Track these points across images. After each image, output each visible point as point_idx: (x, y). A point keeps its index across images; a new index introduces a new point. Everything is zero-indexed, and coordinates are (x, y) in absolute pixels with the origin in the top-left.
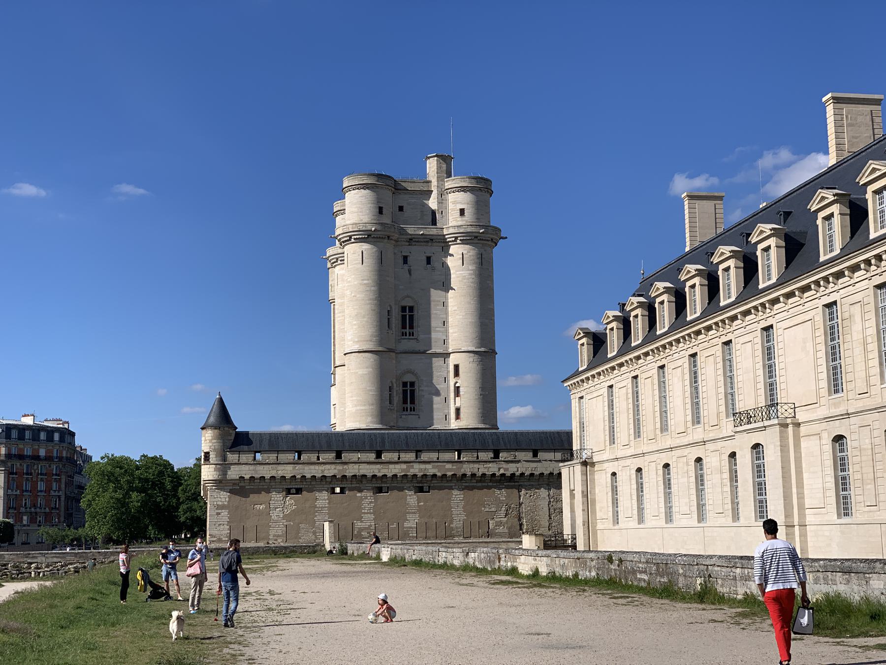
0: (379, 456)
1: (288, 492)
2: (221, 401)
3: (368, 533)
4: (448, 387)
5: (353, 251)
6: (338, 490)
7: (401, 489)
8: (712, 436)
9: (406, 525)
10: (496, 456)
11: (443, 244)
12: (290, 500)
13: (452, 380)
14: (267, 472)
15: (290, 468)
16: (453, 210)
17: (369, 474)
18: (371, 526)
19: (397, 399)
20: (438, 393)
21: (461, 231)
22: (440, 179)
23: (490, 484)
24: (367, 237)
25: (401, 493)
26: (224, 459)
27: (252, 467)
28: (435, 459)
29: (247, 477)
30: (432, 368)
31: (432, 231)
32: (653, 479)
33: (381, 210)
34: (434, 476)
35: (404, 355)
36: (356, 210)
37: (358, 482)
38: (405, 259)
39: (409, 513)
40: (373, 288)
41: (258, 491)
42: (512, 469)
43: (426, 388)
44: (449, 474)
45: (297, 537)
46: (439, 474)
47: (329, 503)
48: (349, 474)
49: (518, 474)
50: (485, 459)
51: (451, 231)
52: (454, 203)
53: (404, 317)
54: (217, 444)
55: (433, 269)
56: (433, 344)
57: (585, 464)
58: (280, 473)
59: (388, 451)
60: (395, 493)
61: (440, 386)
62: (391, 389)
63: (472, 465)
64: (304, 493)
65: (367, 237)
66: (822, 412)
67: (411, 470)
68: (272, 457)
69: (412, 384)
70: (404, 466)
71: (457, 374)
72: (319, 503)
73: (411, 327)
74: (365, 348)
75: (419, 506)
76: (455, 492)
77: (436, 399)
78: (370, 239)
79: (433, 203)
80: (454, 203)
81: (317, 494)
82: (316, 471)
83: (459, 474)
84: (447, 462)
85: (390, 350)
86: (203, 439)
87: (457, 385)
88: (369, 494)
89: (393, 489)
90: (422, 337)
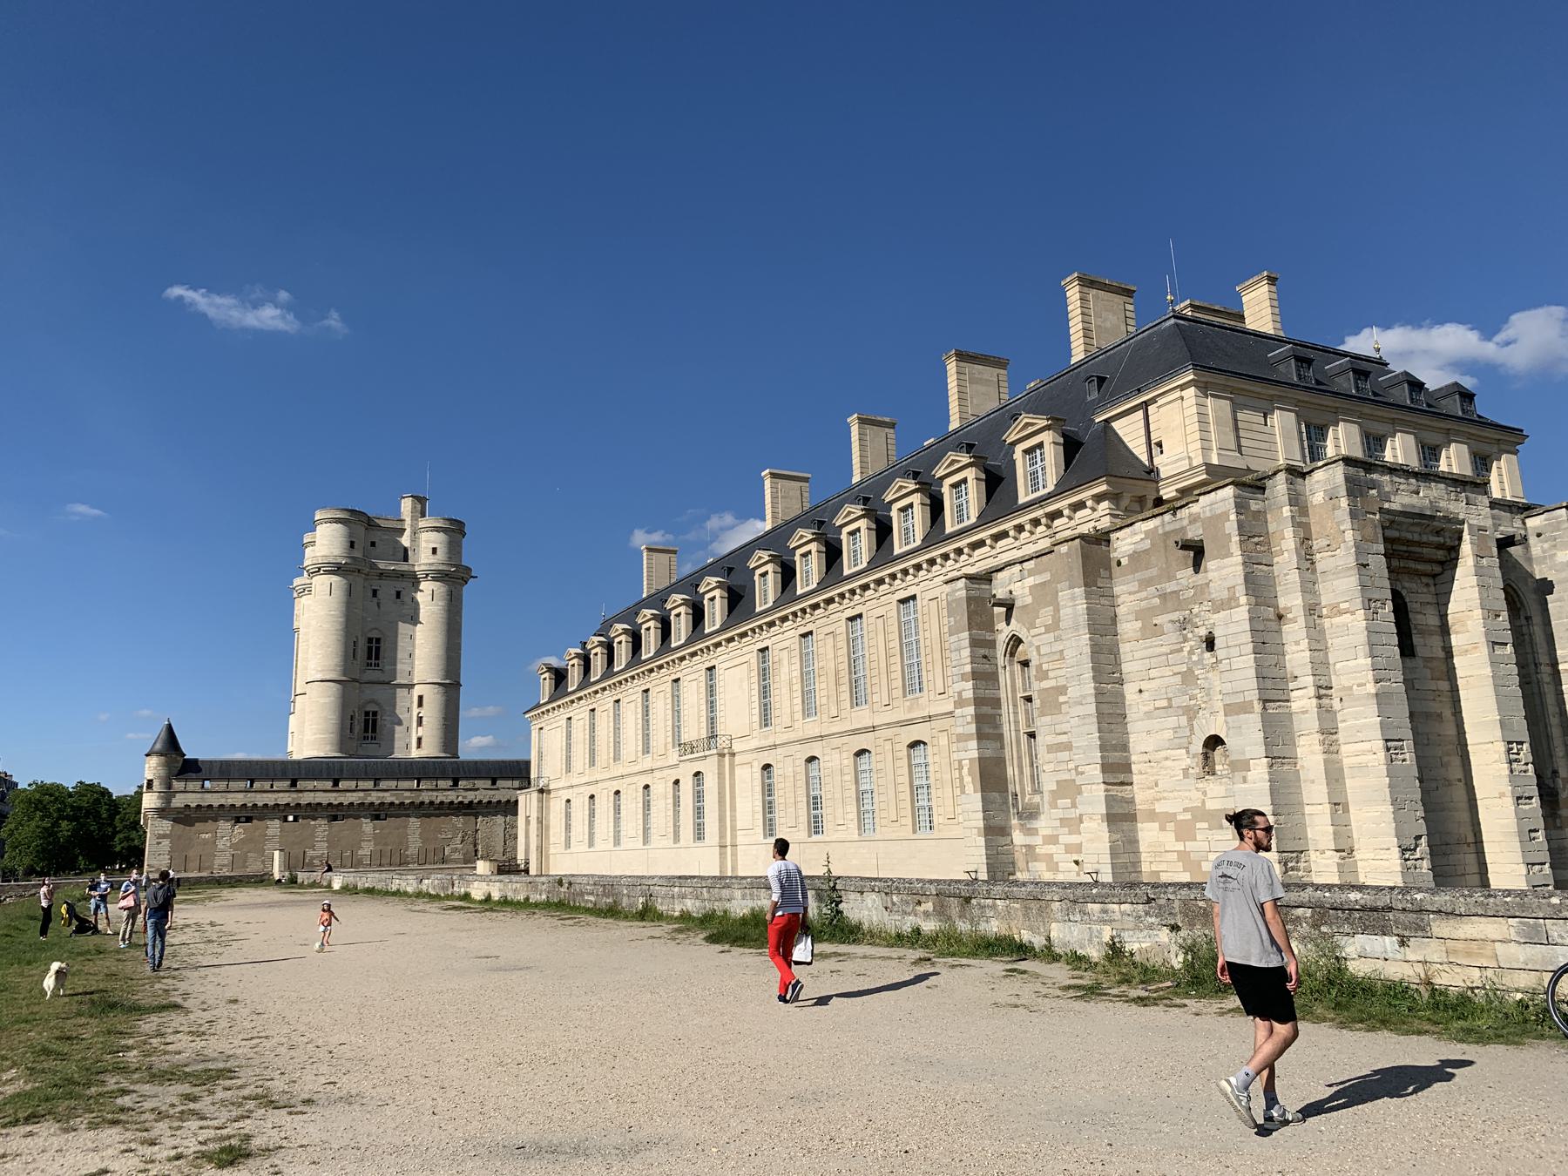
0: (336, 783)
1: (238, 820)
2: (170, 728)
5: (322, 583)
6: (291, 818)
7: (357, 817)
8: (659, 764)
10: (455, 784)
11: (414, 580)
12: (239, 829)
13: (415, 710)
14: (215, 800)
15: (241, 795)
17: (325, 802)
19: (358, 728)
20: (400, 723)
22: (414, 518)
24: (338, 569)
31: (404, 567)
32: (604, 805)
33: (352, 545)
34: (392, 804)
37: (314, 810)
38: (375, 593)
42: (471, 796)
48: (303, 802)
53: (370, 649)
54: (162, 772)
55: (403, 603)
57: (541, 791)
58: (230, 802)
60: (351, 820)
66: (754, 743)
71: (420, 704)
72: (270, 832)
73: (377, 658)
77: (397, 728)
79: (405, 541)
82: (270, 799)
83: (417, 802)
85: (354, 680)
90: (387, 668)
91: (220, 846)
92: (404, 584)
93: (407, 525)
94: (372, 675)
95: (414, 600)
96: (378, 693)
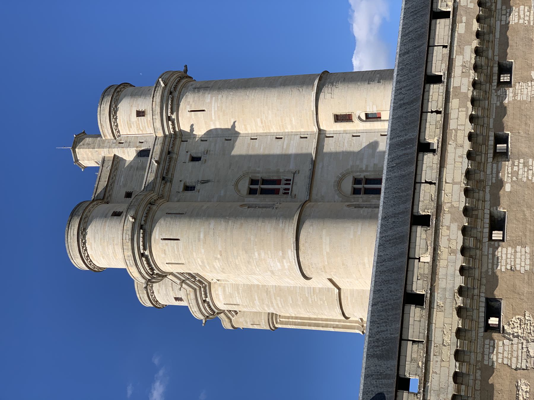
4: (367, 132)
5: (163, 255)
6: (497, 235)
7: (502, 110)
11: (175, 140)
12: (510, 320)
15: (438, 318)
16: (138, 128)
17: (465, 164)
24: (143, 230)
25: (510, 111)
28: (446, 51)
31: (158, 149)
33: (117, 214)
34: (477, 51)
35: (314, 192)
36: (110, 247)
37: (481, 184)
38: (188, 188)
40: (212, 226)
43: (365, 162)
44: (476, 26)
46: (475, 43)
47: (524, 245)
48: (461, 202)
51: (158, 124)
56: (304, 151)
58: (450, 338)
59: (421, 129)
60: (507, 120)
61: (364, 142)
64: (497, 294)
65: (143, 230)
67: (464, 89)
68: (413, 353)
69: (357, 181)
70: (454, 103)
73: (278, 182)
74: (293, 240)
76: (513, 19)
78: (147, 227)
79: (129, 155)
80: (130, 127)
81: (502, 267)
82: (451, 264)
84: (453, 30)
85: (303, 206)
87: (363, 117)
88: (507, 169)
89: (501, 126)
90: (292, 167)
92: (182, 153)
93: (108, 153)
94: (300, 187)
95: (203, 140)
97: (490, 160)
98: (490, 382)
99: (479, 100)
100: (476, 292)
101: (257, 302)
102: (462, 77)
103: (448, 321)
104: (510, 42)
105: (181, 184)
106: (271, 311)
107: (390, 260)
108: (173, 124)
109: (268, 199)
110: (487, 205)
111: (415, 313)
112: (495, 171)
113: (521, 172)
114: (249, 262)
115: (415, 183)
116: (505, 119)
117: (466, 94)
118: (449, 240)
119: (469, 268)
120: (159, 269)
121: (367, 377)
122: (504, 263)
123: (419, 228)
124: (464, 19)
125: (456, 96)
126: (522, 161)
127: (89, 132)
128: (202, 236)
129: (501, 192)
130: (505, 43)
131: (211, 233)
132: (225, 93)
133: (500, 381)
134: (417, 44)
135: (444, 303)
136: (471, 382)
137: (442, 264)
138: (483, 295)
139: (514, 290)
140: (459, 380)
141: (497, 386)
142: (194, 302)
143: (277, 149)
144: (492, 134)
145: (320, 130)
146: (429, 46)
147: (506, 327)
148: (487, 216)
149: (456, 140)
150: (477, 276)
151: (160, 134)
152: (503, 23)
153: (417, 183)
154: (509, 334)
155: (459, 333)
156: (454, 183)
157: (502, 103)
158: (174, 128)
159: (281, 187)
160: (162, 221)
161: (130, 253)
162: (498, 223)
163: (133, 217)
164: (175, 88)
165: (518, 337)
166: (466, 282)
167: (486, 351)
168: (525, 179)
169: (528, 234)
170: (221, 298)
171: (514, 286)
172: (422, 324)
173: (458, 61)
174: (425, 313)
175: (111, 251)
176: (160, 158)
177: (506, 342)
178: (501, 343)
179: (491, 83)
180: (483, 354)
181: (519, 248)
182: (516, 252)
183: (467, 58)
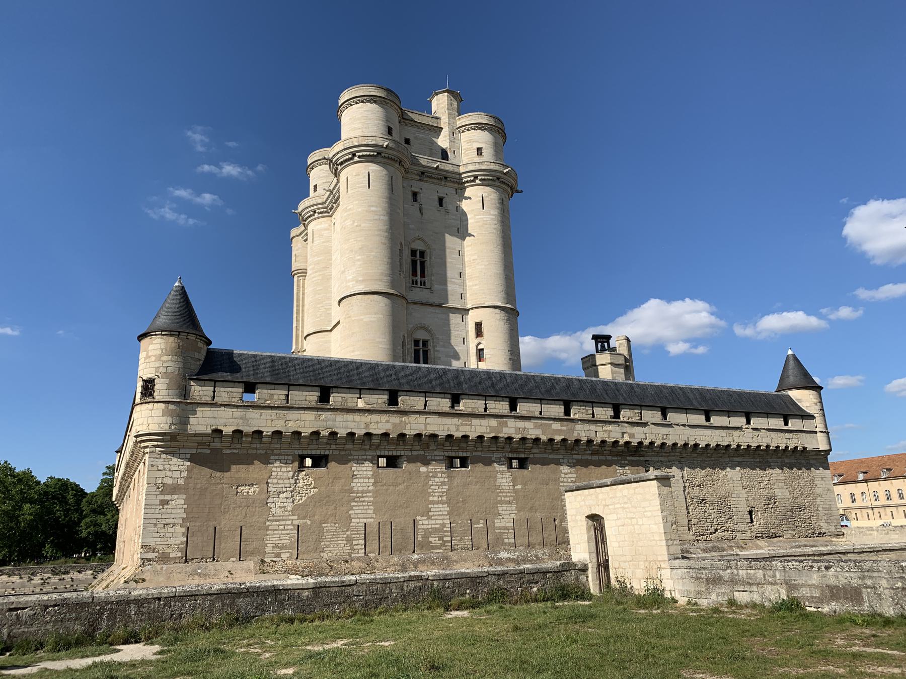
2: (183, 292)
3: (441, 538)
4: (468, 350)
6: (383, 462)
7: (488, 462)
9: (498, 523)
11: (456, 183)
12: (309, 478)
15: (309, 416)
16: (467, 150)
17: (442, 434)
18: (443, 525)
21: (484, 167)
23: (609, 458)
24: (376, 155)
25: (488, 468)
26: (185, 392)
27: (238, 413)
28: (537, 414)
29: (228, 430)
30: (449, 325)
33: (390, 131)
34: (537, 440)
35: (415, 306)
36: (360, 125)
37: (426, 447)
38: (415, 195)
39: (501, 502)
40: (382, 217)
41: (247, 460)
42: (637, 435)
44: (558, 438)
45: (318, 549)
46: (544, 438)
47: (374, 484)
48: (410, 431)
49: (646, 442)
50: (603, 418)
51: (470, 168)
52: (470, 141)
53: (414, 263)
54: (170, 364)
56: (450, 297)
58: (292, 426)
59: (471, 396)
60: (480, 467)
61: (459, 348)
62: (403, 345)
63: (587, 427)
64: (332, 465)
65: (376, 155)
67: (505, 430)
68: (278, 395)
69: (425, 343)
70: (494, 422)
71: (479, 332)
73: (423, 275)
74: (373, 289)
75: (515, 491)
76: (564, 469)
78: (379, 159)
79: (443, 141)
81: (355, 467)
82: (357, 425)
83: (571, 439)
84: (555, 419)
85: (403, 297)
86: (142, 355)
87: (480, 347)
88: (440, 468)
89: (476, 460)
90: (436, 287)
91: (275, 510)
93: (444, 123)
94: (419, 294)
96: (428, 317)
97: (446, 454)
98: (256, 462)
99: (496, 443)
100: (333, 446)
101: (316, 259)
102: (516, 428)
103: (307, 424)
104: (545, 467)
105: (418, 191)
106: (309, 272)
107: (358, 373)
108: (471, 181)
109: (407, 267)
110: (408, 453)
111: (312, 396)
112: (438, 458)
113: (437, 479)
114: (351, 251)
115: (425, 393)
116: (481, 465)
117: (501, 432)
118: (377, 422)
119: (354, 440)
120: (342, 170)
121: (255, 356)
122: (359, 468)
123: (386, 397)
124: (564, 428)
125: (499, 423)
126: (446, 480)
127: (462, 106)
128: (373, 209)
129: (419, 464)
130: (544, 462)
131: (376, 217)
132: (499, 227)
133: (257, 470)
134: (543, 390)
135: (323, 420)
136: (254, 446)
137: (357, 417)
138: (331, 452)
139: (336, 478)
140: (256, 436)
141: (251, 468)
142: (313, 202)
143: (451, 273)
144: (468, 454)
145: (469, 310)
146: (541, 400)
147: (304, 473)
148: (398, 453)
149: (462, 425)
150: (347, 446)
151: (462, 170)
152: (561, 461)
153: (425, 394)
154: (298, 476)
155: (297, 434)
156: (426, 425)
157: (494, 462)
158: (467, 182)
159: (419, 278)
160: (385, 172)
161: (355, 144)
162: (393, 462)
163: (387, 146)
164: (503, 182)
165: (296, 483)
166: (341, 438)
167: (281, 458)
168: (430, 483)
169: (385, 487)
170: (318, 227)
171: (339, 478)
172: (304, 402)
173: (529, 424)
174: (313, 404)
175: (356, 126)
176: (441, 170)
177: (291, 474)
178: (290, 469)
179: (511, 452)
180: (280, 455)
181: (372, 480)
182: (369, 478)
183: (531, 432)
